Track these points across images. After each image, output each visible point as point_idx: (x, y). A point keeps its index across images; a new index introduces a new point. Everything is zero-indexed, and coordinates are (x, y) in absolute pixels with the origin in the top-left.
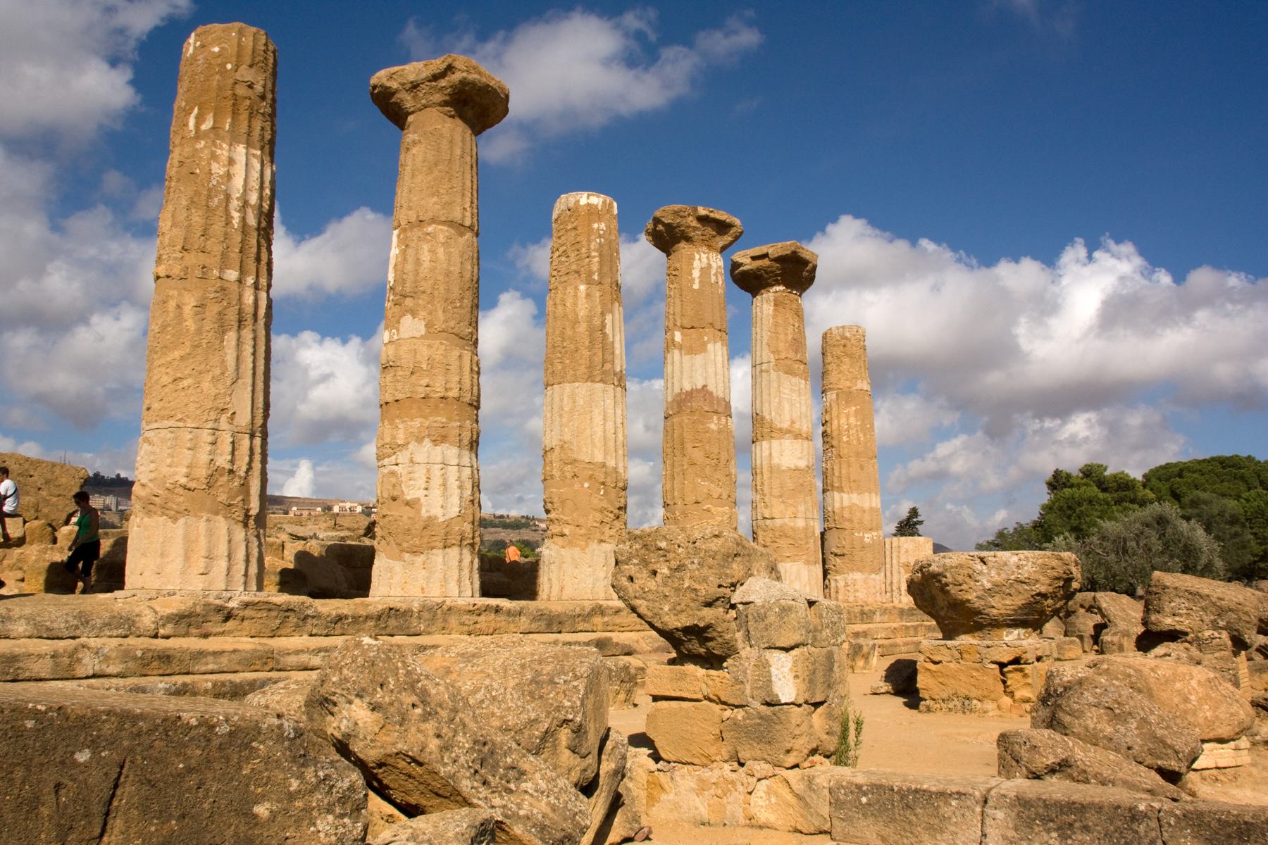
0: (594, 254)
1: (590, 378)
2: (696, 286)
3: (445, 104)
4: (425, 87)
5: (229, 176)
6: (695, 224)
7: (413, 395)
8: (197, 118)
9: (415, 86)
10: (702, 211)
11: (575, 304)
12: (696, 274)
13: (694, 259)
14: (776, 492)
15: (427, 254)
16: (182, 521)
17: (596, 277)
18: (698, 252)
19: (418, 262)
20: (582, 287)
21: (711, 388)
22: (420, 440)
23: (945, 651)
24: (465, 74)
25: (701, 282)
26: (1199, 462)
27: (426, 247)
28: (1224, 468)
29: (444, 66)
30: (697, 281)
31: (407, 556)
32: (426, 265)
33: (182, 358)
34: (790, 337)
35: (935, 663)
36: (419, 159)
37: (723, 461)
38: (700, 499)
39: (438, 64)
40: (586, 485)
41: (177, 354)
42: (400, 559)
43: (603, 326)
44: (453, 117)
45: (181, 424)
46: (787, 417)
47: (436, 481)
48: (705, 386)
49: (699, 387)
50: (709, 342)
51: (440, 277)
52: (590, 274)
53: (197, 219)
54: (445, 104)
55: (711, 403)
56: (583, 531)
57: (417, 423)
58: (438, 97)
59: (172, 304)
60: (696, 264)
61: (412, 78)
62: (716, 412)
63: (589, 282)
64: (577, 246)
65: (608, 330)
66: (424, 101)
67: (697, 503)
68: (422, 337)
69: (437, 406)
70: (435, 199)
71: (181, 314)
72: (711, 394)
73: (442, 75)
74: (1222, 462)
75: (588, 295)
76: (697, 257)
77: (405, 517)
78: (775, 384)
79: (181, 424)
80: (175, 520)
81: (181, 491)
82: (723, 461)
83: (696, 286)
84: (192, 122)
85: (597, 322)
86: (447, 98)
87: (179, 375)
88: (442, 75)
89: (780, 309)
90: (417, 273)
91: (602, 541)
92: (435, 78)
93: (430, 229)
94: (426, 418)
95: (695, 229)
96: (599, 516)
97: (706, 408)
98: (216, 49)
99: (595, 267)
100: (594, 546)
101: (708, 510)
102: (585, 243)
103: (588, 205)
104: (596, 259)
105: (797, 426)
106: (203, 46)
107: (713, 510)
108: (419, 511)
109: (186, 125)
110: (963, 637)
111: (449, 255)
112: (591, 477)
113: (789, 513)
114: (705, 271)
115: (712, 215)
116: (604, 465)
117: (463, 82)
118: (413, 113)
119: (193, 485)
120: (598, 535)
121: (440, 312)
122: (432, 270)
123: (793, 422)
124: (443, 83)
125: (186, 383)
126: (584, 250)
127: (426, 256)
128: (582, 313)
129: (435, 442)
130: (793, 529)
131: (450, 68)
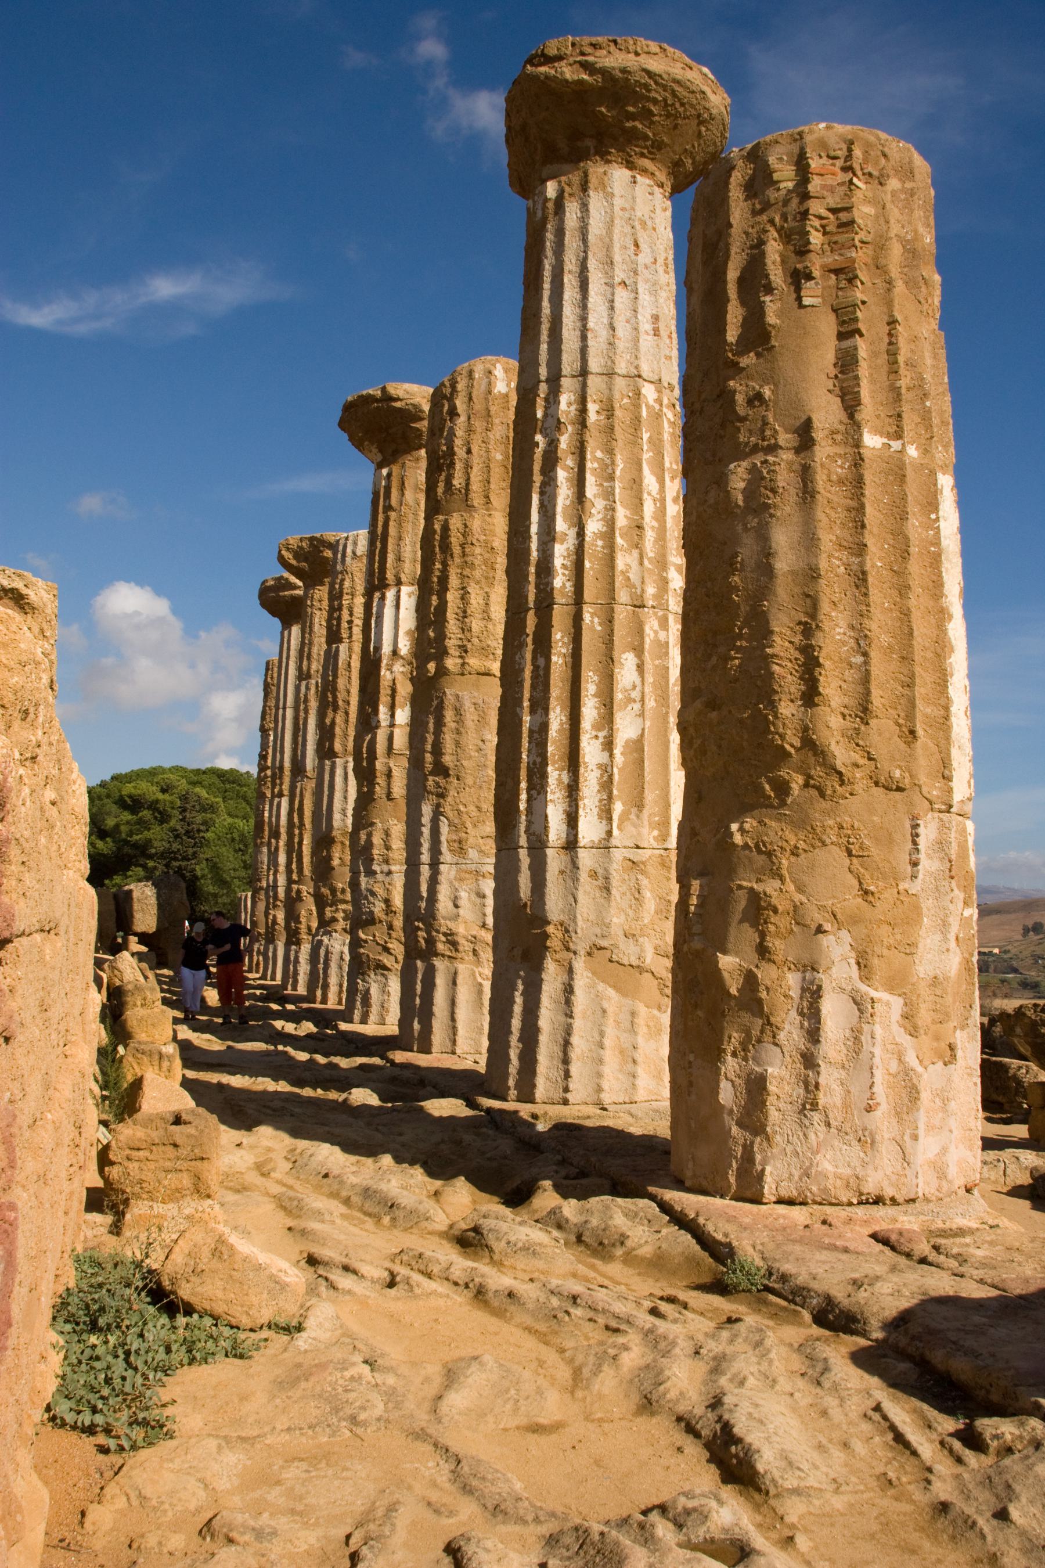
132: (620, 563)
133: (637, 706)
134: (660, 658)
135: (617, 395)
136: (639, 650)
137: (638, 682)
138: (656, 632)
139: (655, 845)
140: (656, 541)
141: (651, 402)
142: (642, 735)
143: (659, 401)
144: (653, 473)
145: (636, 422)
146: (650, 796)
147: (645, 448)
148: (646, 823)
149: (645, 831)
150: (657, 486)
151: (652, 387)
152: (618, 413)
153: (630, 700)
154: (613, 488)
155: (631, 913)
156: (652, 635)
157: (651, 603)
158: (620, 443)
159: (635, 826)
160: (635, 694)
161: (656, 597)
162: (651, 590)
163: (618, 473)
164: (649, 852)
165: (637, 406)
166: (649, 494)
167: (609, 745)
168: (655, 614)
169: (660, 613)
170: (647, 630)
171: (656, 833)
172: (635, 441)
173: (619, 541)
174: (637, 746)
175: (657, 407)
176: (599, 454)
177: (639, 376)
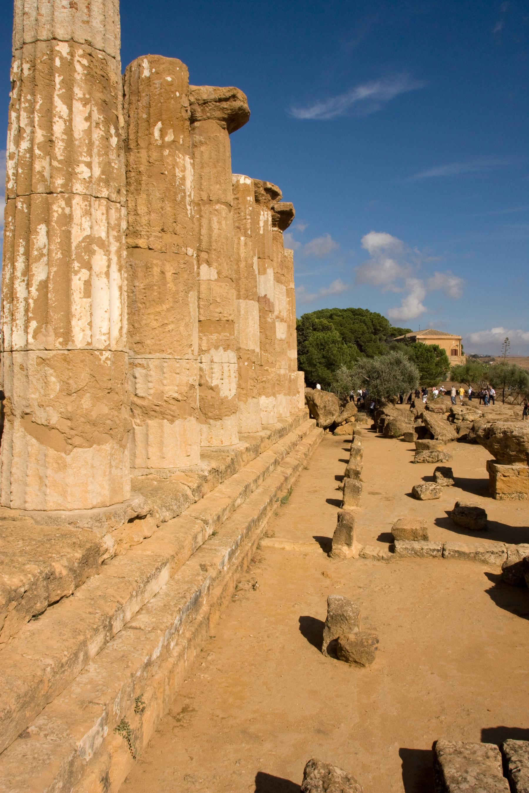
0: (248, 217)
1: (247, 298)
2: (261, 232)
3: (224, 119)
4: (211, 105)
5: (183, 179)
6: (263, 192)
7: (212, 318)
8: (161, 130)
9: (205, 102)
10: (269, 185)
11: (238, 249)
12: (261, 224)
13: (260, 214)
15: (216, 224)
16: (177, 422)
17: (249, 232)
18: (263, 210)
19: (210, 228)
20: (242, 238)
21: (268, 296)
22: (217, 348)
23: (511, 471)
24: (242, 103)
25: (264, 229)
26: (341, 311)
27: (215, 219)
28: (354, 315)
29: (228, 95)
30: (262, 229)
31: (211, 421)
32: (216, 231)
33: (168, 310)
34: (279, 260)
35: (504, 476)
36: (206, 156)
38: (263, 364)
39: (224, 91)
40: (246, 364)
41: (165, 307)
42: (206, 422)
44: (224, 128)
45: (170, 356)
47: (226, 374)
48: (266, 295)
51: (224, 241)
52: (246, 230)
53: (169, 209)
54: (224, 119)
56: (245, 392)
57: (215, 336)
58: (218, 114)
59: (156, 270)
60: (261, 217)
61: (205, 97)
63: (245, 235)
64: (238, 211)
66: (208, 114)
68: (216, 280)
69: (224, 326)
70: (218, 186)
71: (165, 278)
72: (269, 300)
73: (226, 100)
74: (354, 312)
75: (246, 243)
76: (262, 213)
77: (209, 397)
79: (170, 356)
80: (172, 422)
81: (172, 402)
83: (261, 232)
84: (157, 134)
86: (226, 116)
87: (166, 322)
88: (226, 100)
89: (275, 242)
90: (210, 236)
92: (220, 100)
93: (218, 207)
94: (219, 333)
95: (263, 195)
97: (267, 309)
98: (169, 79)
99: (248, 226)
100: (250, 400)
101: (267, 370)
102: (243, 209)
103: (245, 184)
104: (249, 221)
105: (282, 314)
106: (157, 73)
107: (269, 370)
108: (218, 393)
109: (152, 134)
110: (517, 464)
111: (226, 225)
112: (248, 358)
114: (266, 222)
115: (273, 188)
117: (240, 109)
118: (200, 120)
119: (180, 398)
121: (225, 264)
122: (219, 236)
123: (280, 312)
124: (225, 105)
125: (170, 327)
126: (242, 214)
127: (215, 226)
128: (242, 255)
129: (225, 350)
131: (234, 97)
132: (37, 167)
133: (45, 259)
134: (66, 225)
135: (39, 55)
136: (47, 222)
137: (47, 243)
138: (63, 209)
139: (60, 347)
140: (65, 148)
141: (65, 54)
142: (48, 277)
143: (72, 54)
144: (64, 103)
145: (51, 72)
146: (55, 316)
147: (58, 86)
148: (52, 333)
149: (51, 338)
150: (67, 111)
151: (66, 44)
152: (39, 67)
153: (42, 255)
154: (34, 117)
155: (42, 391)
156: (60, 211)
157: (59, 190)
158: (40, 87)
159: (45, 336)
160: (45, 251)
161: (63, 186)
162: (59, 181)
163: (38, 107)
164: (54, 352)
165: (52, 60)
166: (60, 117)
167: (28, 285)
168: (63, 197)
169: (66, 195)
170: (55, 207)
171: (61, 340)
172: (51, 86)
173: (37, 152)
174: (44, 285)
175: (69, 57)
176: (29, 97)
177: (55, 39)
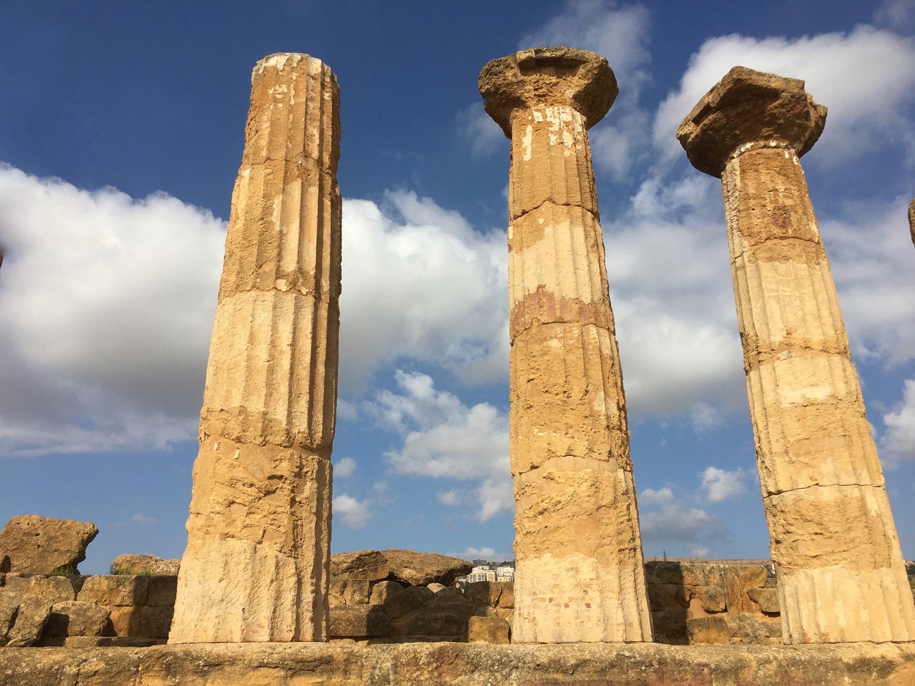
14: (777, 447)
21: (550, 288)
37: (576, 393)
43: (267, 211)
46: (780, 325)
49: (533, 290)
50: (546, 224)
55: (552, 308)
62: (560, 321)
65: (275, 218)
67: (533, 467)
72: (551, 296)
78: (753, 283)
82: (576, 393)
85: (258, 212)
91: (226, 536)
96: (226, 492)
97: (544, 319)
99: (264, 142)
113: (803, 480)
116: (243, 410)
120: (222, 528)
130: (816, 506)
